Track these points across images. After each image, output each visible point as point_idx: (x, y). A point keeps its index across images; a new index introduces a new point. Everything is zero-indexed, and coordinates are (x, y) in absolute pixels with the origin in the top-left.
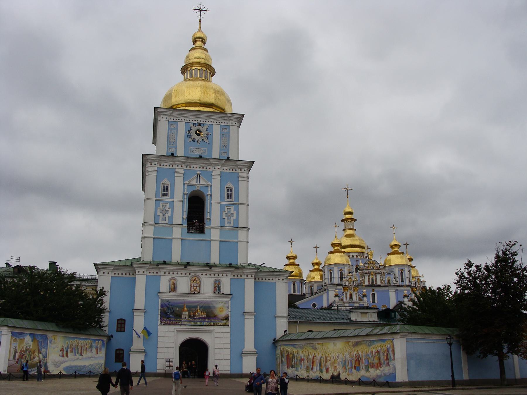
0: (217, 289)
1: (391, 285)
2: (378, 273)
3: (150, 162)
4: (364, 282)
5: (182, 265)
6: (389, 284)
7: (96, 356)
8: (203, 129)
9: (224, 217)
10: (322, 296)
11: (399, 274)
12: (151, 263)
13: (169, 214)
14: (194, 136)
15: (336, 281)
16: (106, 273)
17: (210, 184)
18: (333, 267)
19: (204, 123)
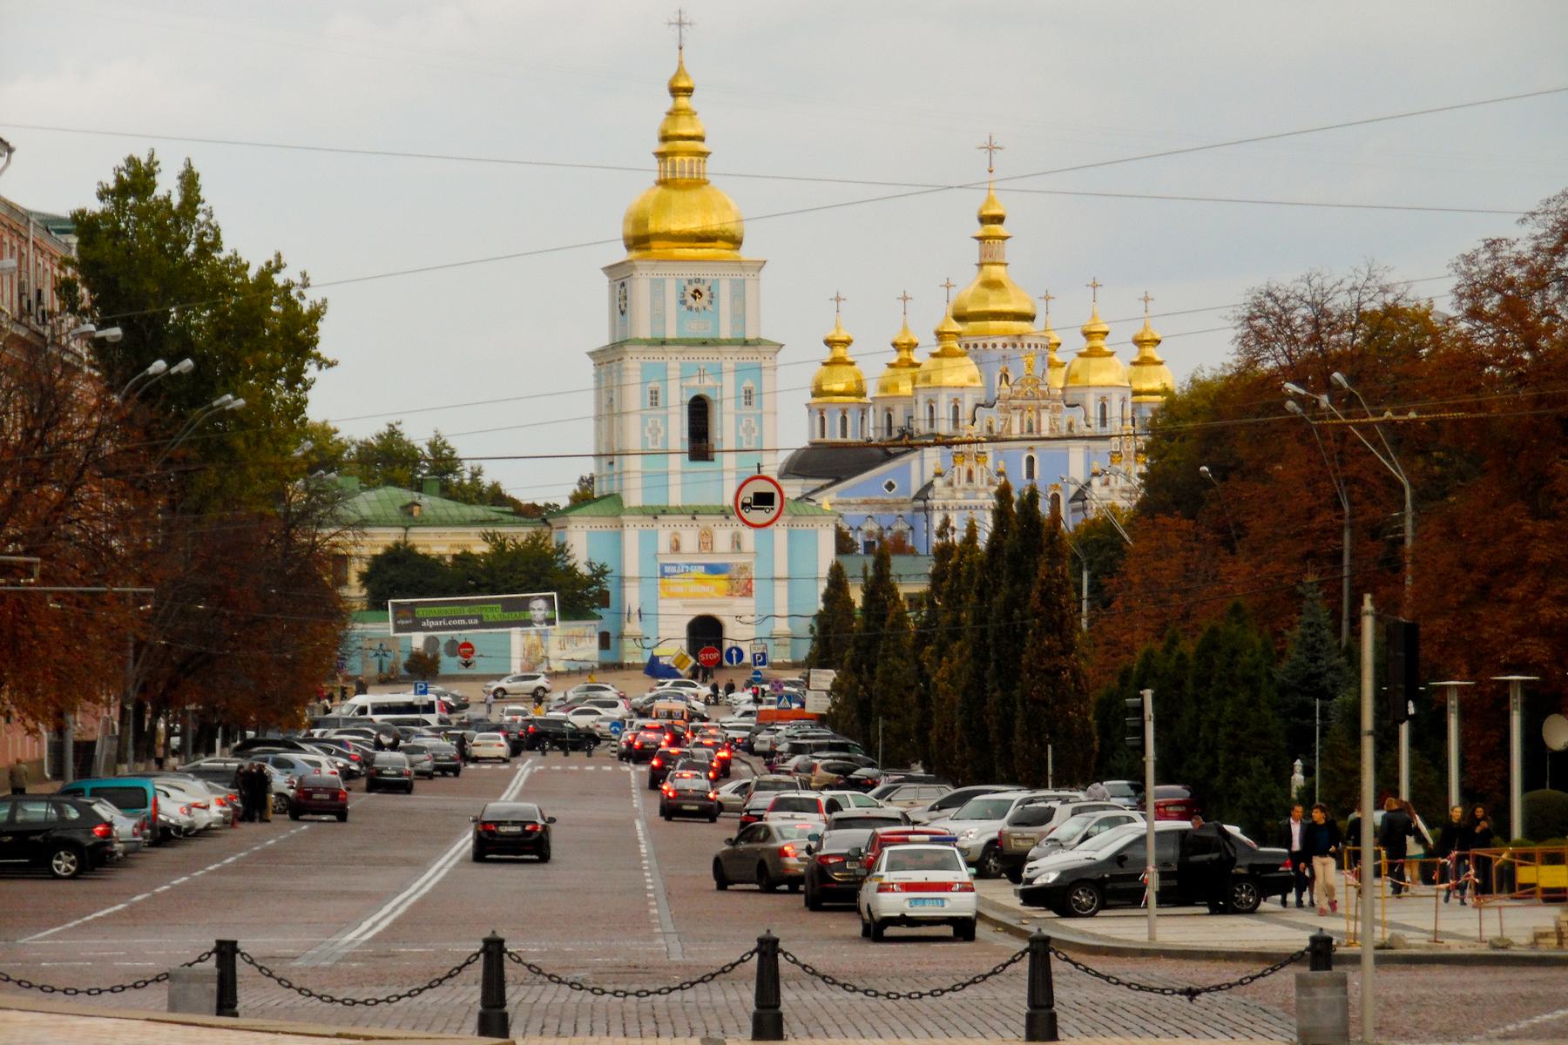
0: (737, 543)
1: (1076, 432)
2: (1046, 407)
3: (630, 355)
4: (1010, 430)
5: (688, 514)
6: (1070, 434)
7: (590, 645)
8: (703, 289)
9: (741, 434)
10: (908, 465)
11: (1096, 411)
12: (643, 511)
13: (662, 434)
14: (691, 301)
15: (944, 428)
16: (579, 526)
17: (719, 384)
18: (937, 395)
19: (706, 277)
